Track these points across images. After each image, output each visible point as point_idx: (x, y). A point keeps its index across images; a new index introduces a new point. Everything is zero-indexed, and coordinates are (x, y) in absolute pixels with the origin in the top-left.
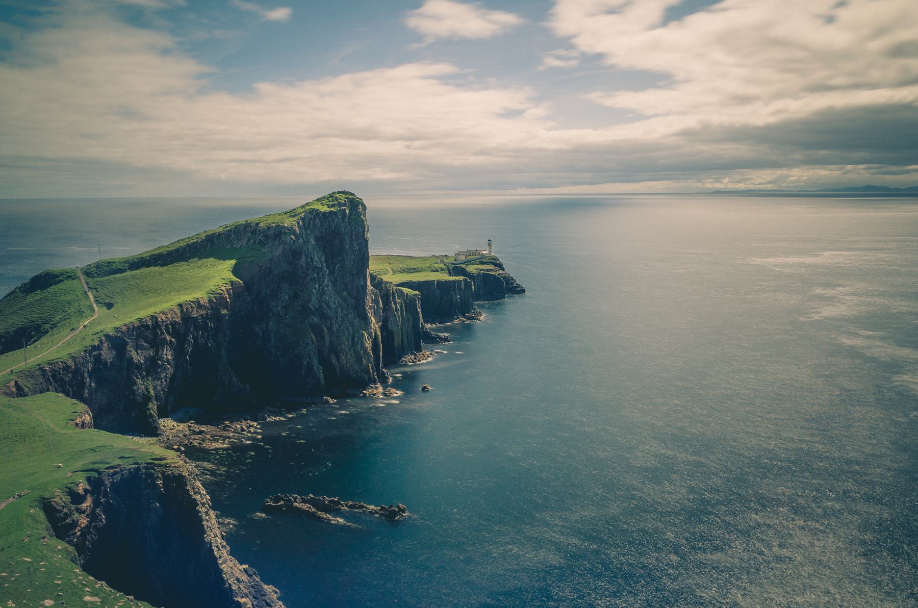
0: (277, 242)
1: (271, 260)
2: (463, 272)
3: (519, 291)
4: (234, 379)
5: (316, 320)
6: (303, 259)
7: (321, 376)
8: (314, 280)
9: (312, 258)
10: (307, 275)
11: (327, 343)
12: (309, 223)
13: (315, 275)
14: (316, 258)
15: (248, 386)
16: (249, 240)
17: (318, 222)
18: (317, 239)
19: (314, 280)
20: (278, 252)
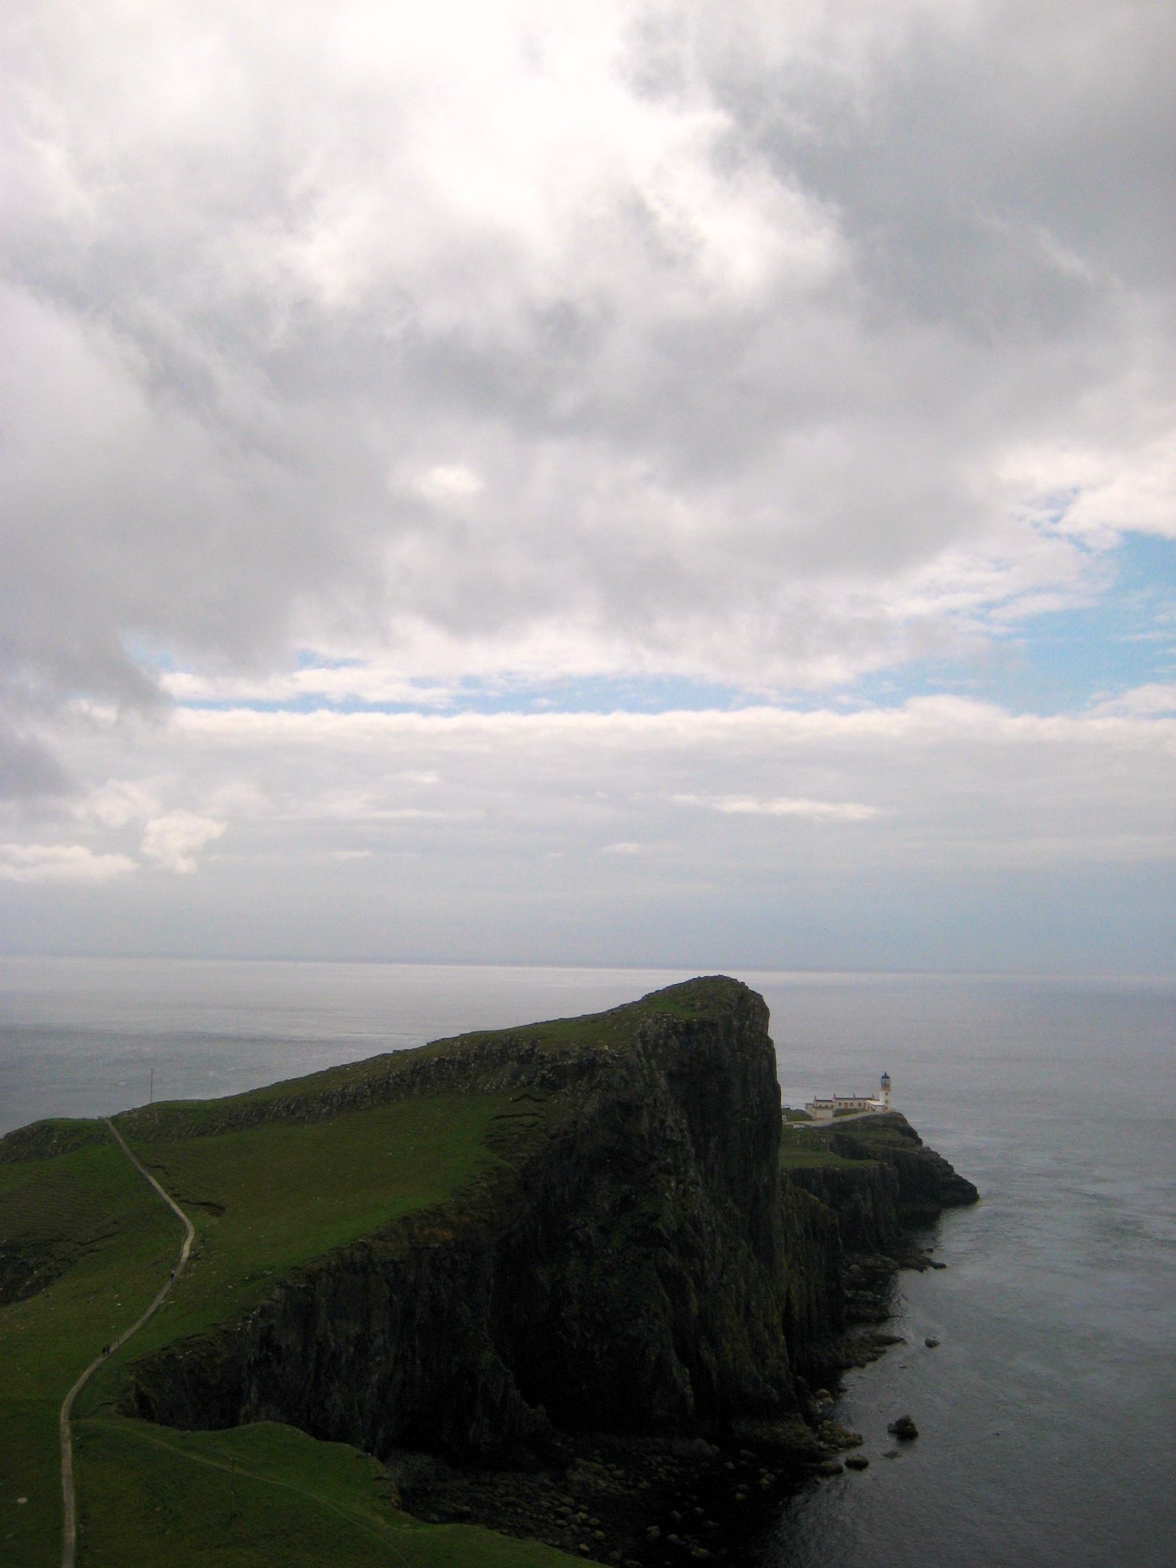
0: (583, 1084)
1: (575, 1123)
2: (856, 1152)
3: (965, 1195)
4: (515, 1393)
5: (672, 1260)
6: (645, 1124)
7: (688, 1390)
8: (666, 1170)
9: (662, 1122)
10: (653, 1158)
11: (695, 1311)
12: (656, 1046)
13: (669, 1160)
14: (670, 1121)
15: (541, 1407)
16: (515, 1077)
17: (674, 1042)
18: (671, 1076)
19: (666, 1170)
20: (592, 1105)
